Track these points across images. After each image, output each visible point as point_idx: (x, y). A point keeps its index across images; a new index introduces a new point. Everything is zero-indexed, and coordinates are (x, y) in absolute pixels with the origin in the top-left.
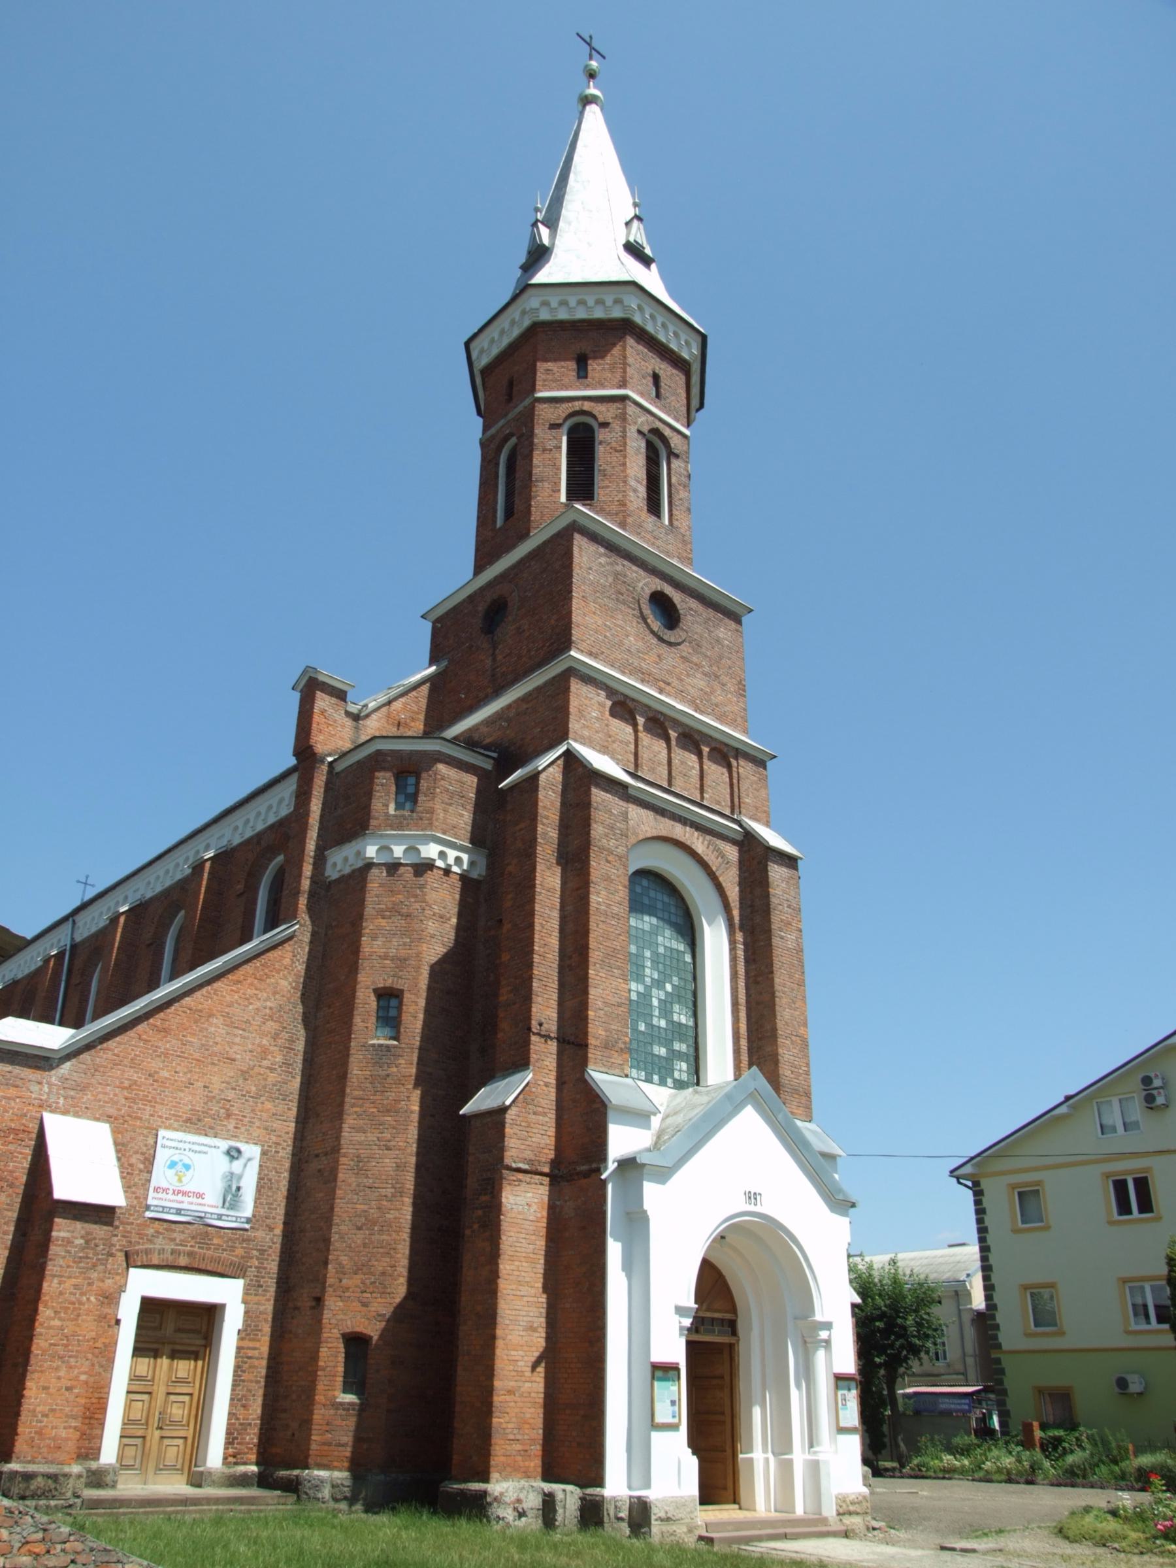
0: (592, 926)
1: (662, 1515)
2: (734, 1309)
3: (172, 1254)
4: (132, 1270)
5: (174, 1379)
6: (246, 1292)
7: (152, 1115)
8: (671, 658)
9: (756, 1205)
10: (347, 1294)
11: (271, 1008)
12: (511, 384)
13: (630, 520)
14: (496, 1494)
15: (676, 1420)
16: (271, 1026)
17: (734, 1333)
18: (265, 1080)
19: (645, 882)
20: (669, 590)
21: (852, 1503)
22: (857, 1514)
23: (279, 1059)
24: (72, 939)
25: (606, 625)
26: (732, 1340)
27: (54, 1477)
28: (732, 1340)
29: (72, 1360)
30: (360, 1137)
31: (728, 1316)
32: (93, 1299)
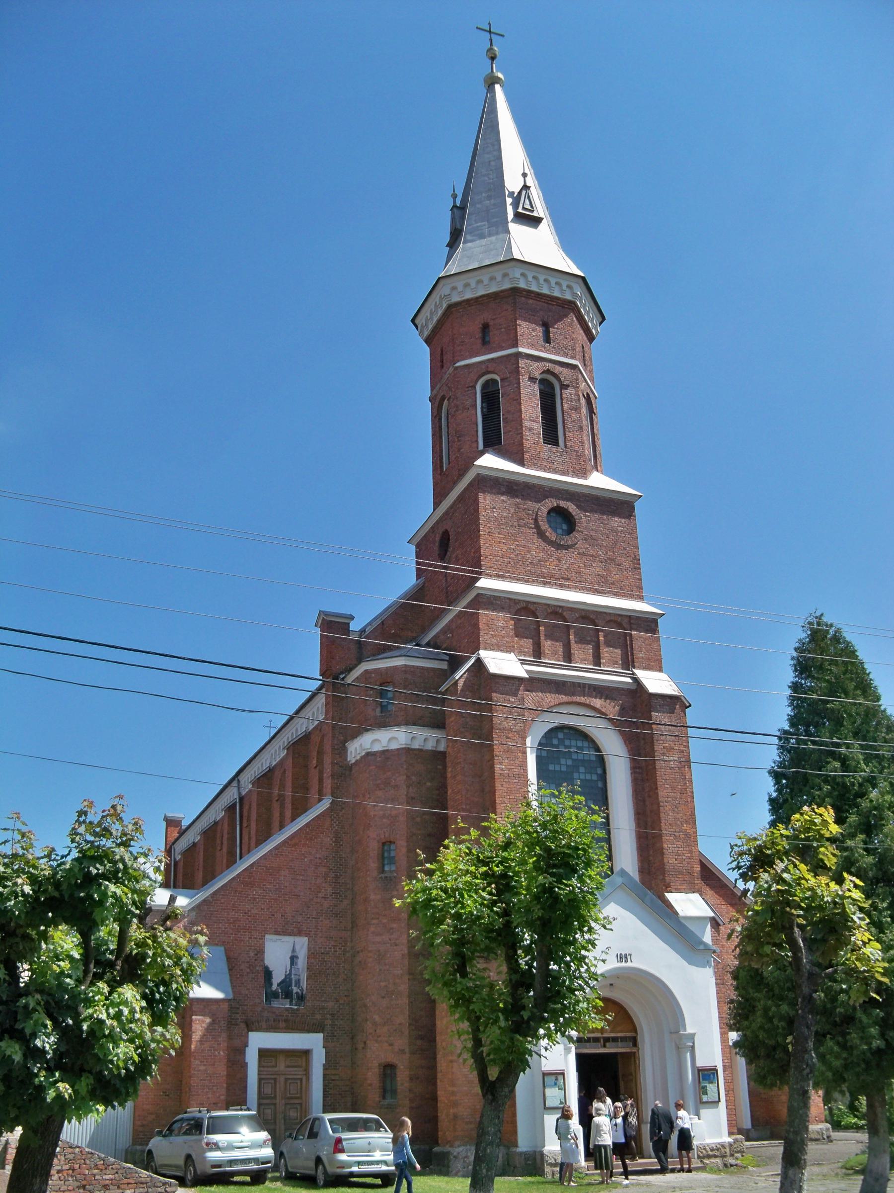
0: (498, 786)
2: (635, 1030)
3: (274, 1021)
4: (250, 1033)
5: (288, 1095)
6: (325, 1040)
7: (250, 938)
8: (569, 558)
9: (626, 962)
10: (379, 1039)
11: (320, 858)
12: (442, 351)
13: (526, 456)
14: (455, 1154)
16: (323, 870)
17: (635, 1044)
18: (322, 905)
19: (561, 735)
20: (563, 504)
21: (712, 1150)
23: (330, 890)
24: (240, 793)
25: (510, 549)
26: (634, 1050)
28: (634, 1050)
29: (215, 1088)
30: (378, 939)
31: (633, 1034)
32: (222, 1053)
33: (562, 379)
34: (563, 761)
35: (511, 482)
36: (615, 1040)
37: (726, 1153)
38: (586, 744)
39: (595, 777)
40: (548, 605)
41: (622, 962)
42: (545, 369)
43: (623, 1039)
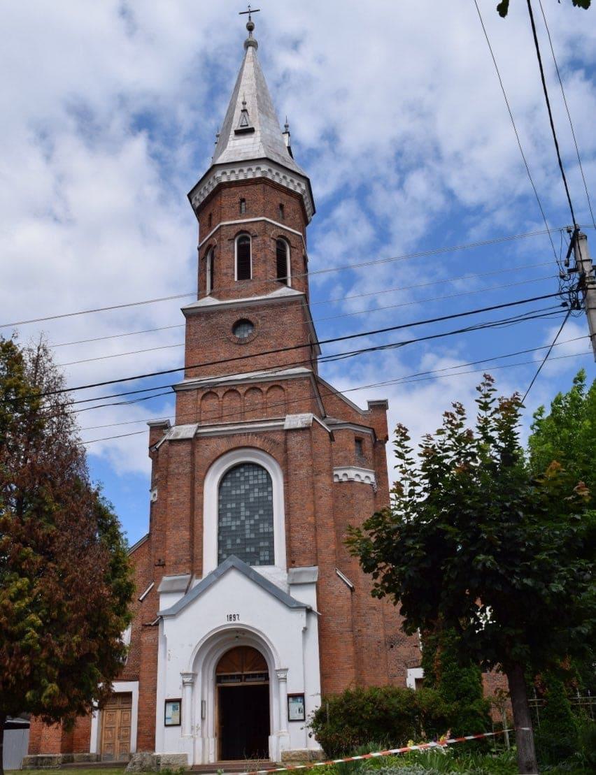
1: (166, 762)
21: (294, 756)
22: (298, 761)
26: (266, 683)
27: (51, 758)
33: (252, 233)
36: (254, 676)
38: (260, 472)
39: (266, 494)
41: (231, 620)
42: (239, 230)
43: (261, 675)
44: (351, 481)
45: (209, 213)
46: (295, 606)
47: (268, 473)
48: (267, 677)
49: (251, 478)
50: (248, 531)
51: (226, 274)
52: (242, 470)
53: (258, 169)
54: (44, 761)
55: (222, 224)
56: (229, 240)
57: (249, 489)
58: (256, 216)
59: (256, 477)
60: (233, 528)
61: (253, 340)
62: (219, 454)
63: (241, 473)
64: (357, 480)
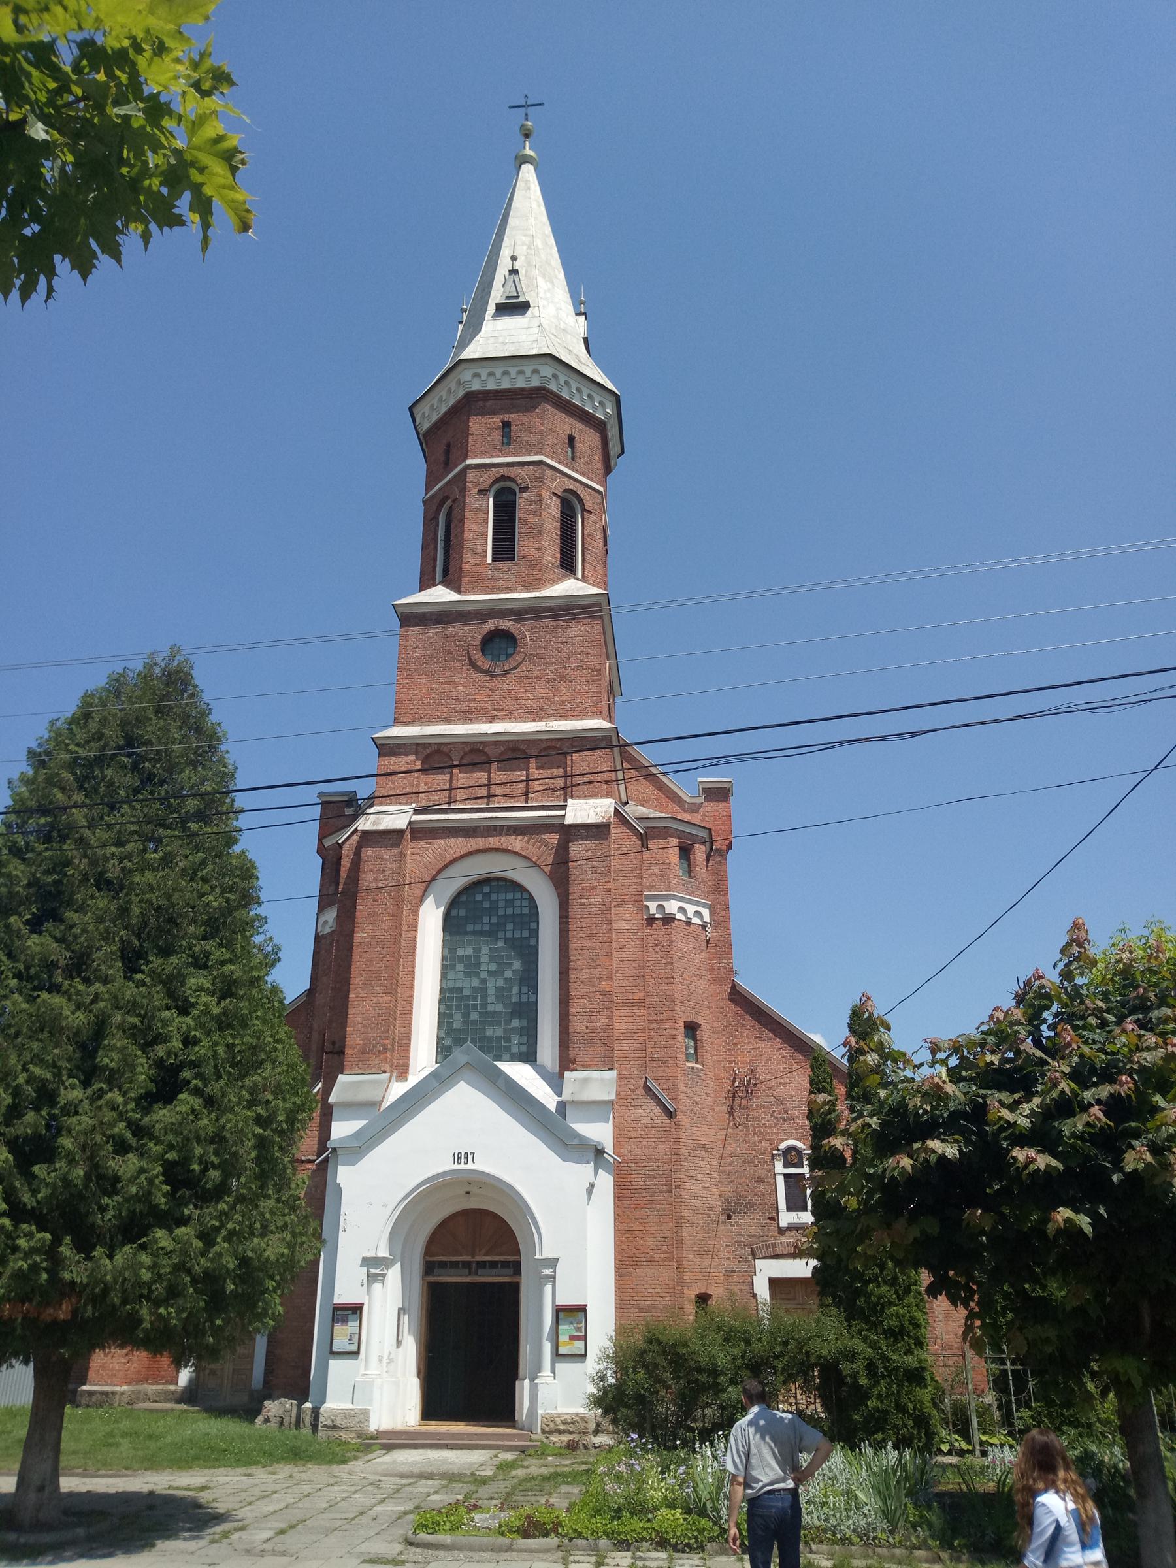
0: (355, 957)
1: (329, 1423)
8: (504, 685)
13: (465, 581)
15: (354, 1348)
21: (564, 1423)
33: (519, 482)
34: (486, 919)
35: (440, 615)
36: (493, 1264)
37: (587, 1428)
38: (518, 895)
39: (526, 934)
40: (467, 743)
42: (498, 475)
43: (505, 1265)
44: (669, 920)
45: (444, 442)
46: (576, 1142)
47: (531, 899)
48: (517, 1268)
49: (502, 904)
50: (491, 999)
51: (473, 550)
52: (487, 889)
53: (535, 372)
54: (94, 1399)
55: (469, 462)
56: (480, 492)
57: (498, 924)
58: (529, 453)
59: (509, 903)
60: (466, 992)
61: (516, 668)
62: (449, 860)
63: (485, 895)
64: (680, 916)
